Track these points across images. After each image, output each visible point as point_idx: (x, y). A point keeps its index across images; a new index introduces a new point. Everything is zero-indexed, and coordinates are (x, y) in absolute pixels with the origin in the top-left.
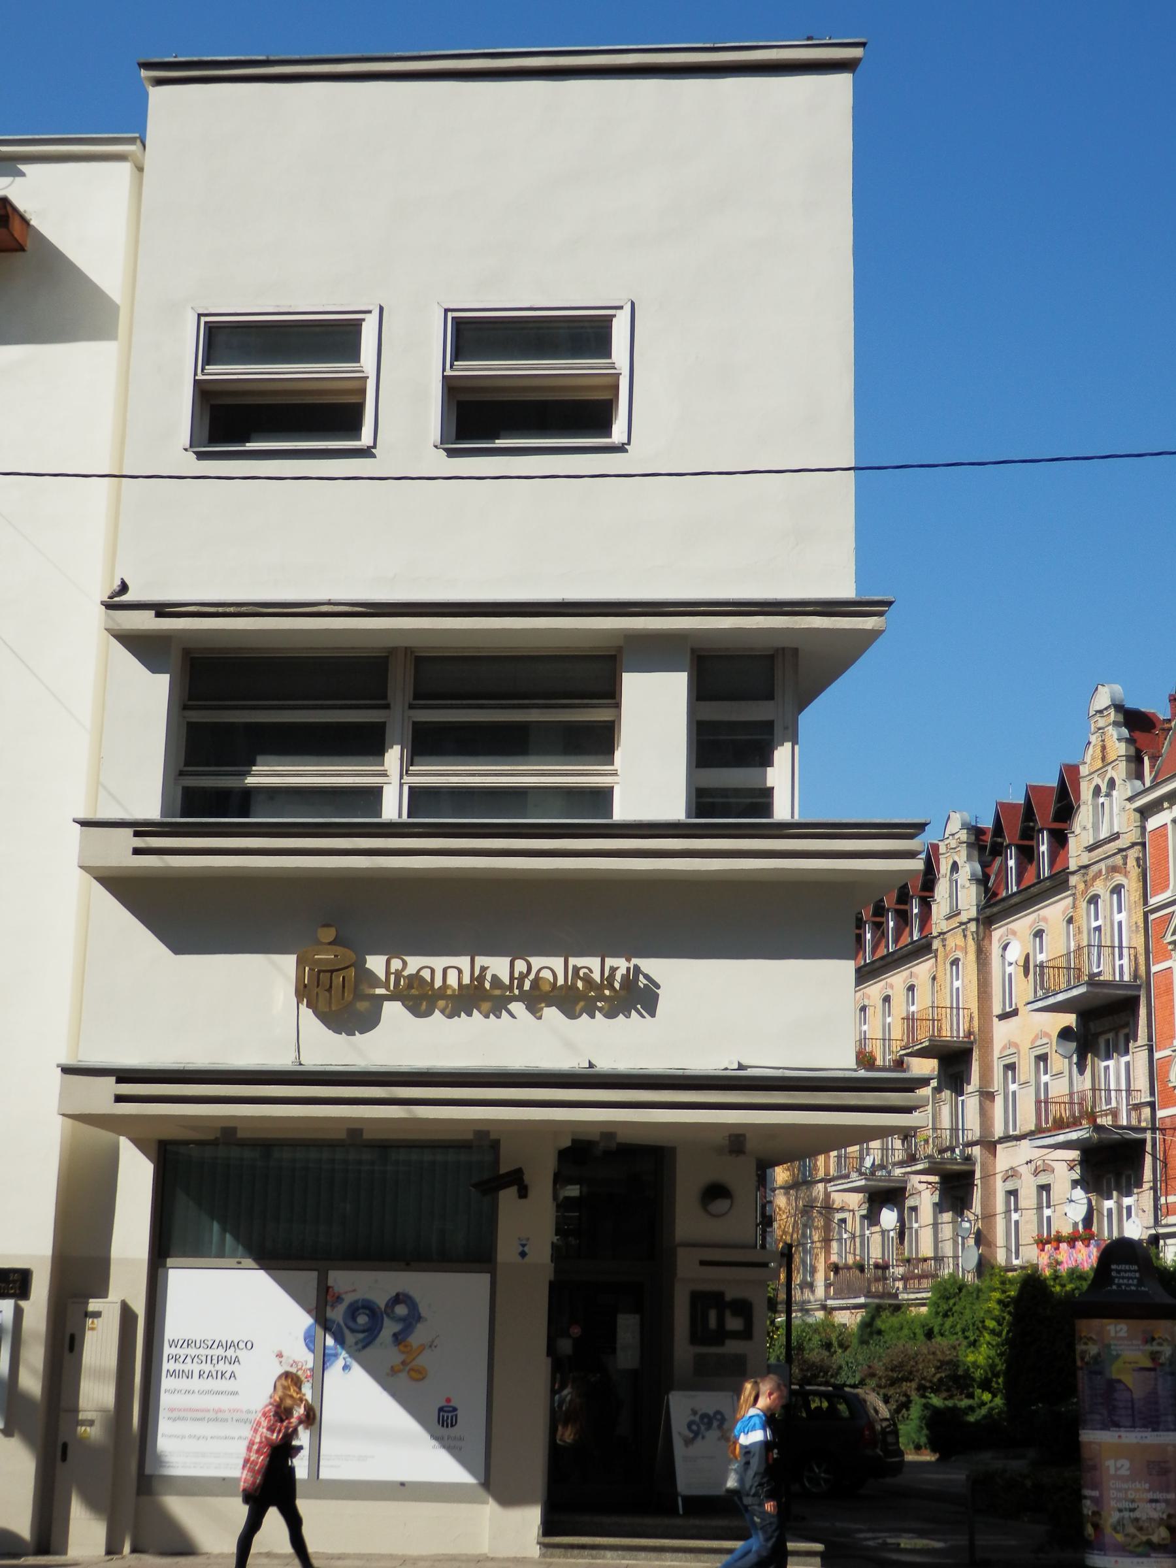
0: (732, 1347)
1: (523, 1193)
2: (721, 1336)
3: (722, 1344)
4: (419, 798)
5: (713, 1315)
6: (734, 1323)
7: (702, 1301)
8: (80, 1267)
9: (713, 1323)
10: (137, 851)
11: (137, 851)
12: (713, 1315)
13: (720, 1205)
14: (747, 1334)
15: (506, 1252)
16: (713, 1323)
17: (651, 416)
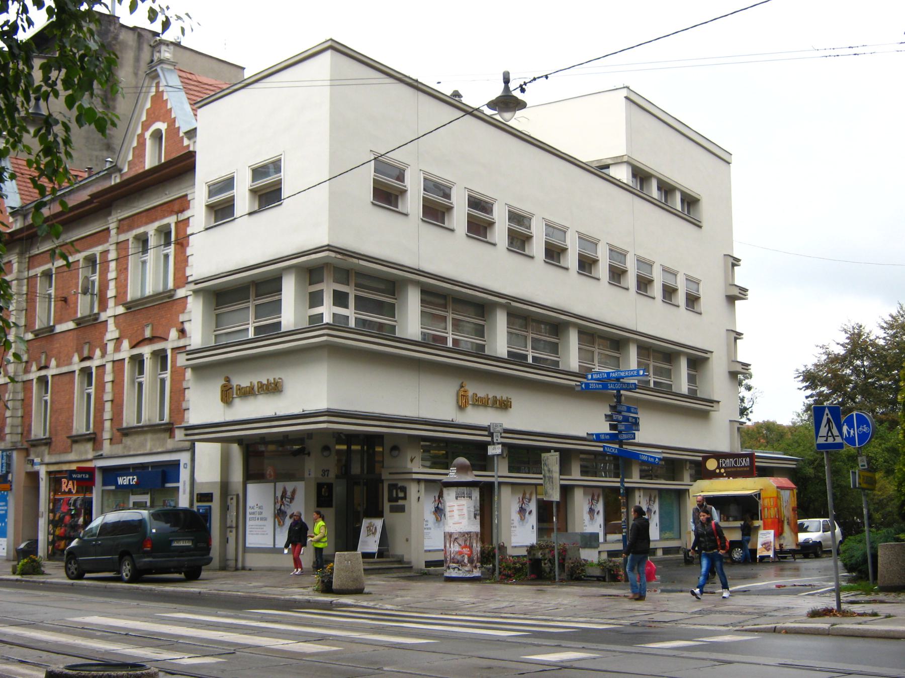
0: (401, 502)
1: (309, 454)
2: (397, 499)
3: (397, 501)
4: (258, 330)
5: (395, 491)
6: (401, 495)
7: (393, 487)
8: (225, 486)
9: (395, 495)
10: (188, 360)
11: (188, 360)
12: (395, 491)
13: (395, 453)
14: (405, 498)
15: (306, 475)
16: (395, 495)
17: (285, 193)
